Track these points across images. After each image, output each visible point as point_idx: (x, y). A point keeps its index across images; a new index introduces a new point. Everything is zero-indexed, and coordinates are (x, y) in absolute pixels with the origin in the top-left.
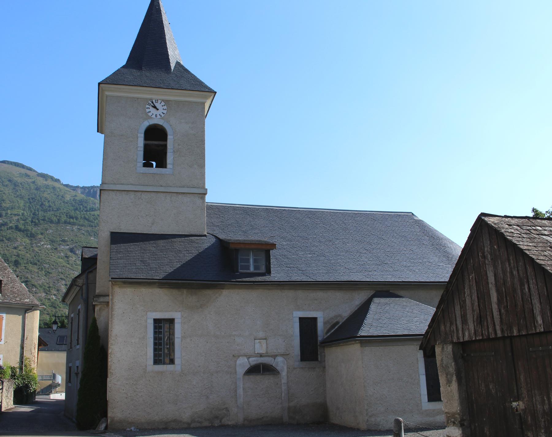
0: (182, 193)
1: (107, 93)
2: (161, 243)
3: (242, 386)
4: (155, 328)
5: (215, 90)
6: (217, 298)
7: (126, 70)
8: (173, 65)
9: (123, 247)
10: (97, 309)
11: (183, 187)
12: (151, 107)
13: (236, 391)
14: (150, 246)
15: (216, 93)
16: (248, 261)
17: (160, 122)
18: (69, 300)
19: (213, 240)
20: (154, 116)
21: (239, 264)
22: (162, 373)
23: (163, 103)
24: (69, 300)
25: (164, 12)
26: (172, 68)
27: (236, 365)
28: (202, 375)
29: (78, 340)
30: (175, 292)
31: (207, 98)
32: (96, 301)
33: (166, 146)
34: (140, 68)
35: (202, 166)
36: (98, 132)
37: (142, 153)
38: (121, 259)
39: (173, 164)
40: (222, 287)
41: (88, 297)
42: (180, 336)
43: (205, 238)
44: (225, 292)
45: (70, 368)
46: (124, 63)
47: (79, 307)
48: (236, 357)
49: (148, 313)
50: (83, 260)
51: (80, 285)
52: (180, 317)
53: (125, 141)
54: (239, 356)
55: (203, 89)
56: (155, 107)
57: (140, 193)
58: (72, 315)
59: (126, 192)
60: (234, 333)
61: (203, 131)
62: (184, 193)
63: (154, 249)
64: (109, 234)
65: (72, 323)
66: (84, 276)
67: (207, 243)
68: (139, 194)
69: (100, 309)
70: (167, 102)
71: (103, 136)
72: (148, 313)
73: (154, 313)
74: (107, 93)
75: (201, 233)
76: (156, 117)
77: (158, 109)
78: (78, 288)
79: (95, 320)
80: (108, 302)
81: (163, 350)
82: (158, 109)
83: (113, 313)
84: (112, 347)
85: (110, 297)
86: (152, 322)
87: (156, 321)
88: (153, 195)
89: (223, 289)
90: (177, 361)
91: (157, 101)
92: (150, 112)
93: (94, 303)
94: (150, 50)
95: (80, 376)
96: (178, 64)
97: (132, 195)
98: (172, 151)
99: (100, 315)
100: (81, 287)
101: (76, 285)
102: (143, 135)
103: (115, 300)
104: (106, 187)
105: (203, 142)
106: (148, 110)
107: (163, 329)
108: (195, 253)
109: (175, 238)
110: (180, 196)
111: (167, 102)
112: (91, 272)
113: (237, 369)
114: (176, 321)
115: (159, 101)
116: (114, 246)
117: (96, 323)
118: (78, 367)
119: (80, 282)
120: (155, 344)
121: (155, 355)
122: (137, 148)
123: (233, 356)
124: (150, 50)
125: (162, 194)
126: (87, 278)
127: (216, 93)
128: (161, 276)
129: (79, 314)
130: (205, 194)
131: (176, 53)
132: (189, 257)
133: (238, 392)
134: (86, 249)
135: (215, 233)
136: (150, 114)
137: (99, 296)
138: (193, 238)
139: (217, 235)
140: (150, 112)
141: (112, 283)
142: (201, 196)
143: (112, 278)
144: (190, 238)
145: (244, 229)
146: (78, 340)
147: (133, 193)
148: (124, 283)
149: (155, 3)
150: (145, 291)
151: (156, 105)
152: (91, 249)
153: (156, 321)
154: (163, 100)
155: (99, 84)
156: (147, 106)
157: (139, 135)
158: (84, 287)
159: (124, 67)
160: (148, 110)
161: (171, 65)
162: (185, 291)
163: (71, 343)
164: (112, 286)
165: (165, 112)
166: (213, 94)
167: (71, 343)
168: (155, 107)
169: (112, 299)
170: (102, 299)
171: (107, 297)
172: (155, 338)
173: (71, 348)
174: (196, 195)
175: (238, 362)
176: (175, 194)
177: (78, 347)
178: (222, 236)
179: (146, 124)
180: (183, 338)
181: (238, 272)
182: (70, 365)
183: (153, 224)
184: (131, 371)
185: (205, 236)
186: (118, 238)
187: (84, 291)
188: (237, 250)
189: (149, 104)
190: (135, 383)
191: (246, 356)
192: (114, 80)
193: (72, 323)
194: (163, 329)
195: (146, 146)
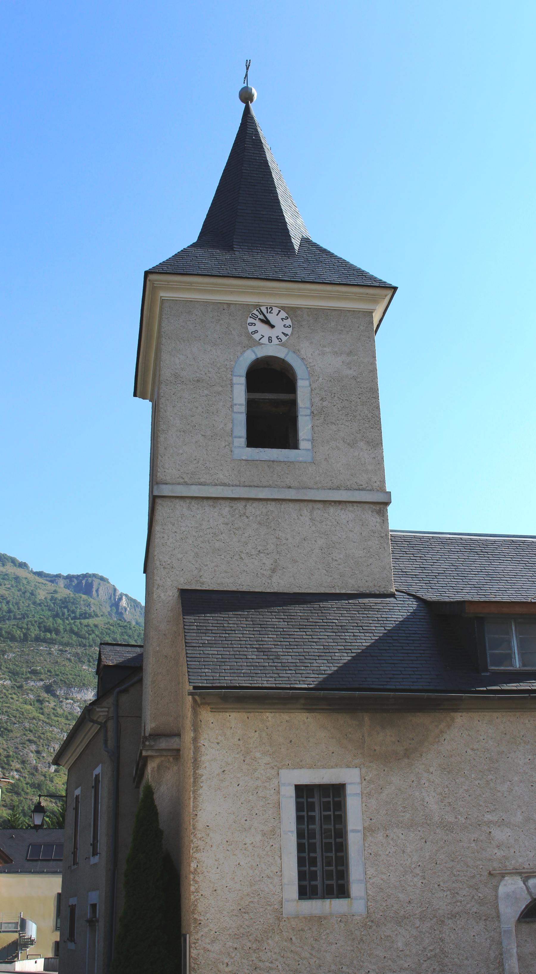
0: (335, 502)
1: (163, 294)
2: (297, 611)
3: (515, 950)
4: (299, 807)
5: (394, 284)
6: (442, 732)
7: (200, 252)
8: (296, 243)
9: (211, 619)
10: (151, 766)
11: (338, 488)
12: (257, 322)
13: (501, 964)
14: (273, 618)
15: (395, 289)
16: (509, 642)
17: (280, 353)
18: (71, 757)
19: (413, 605)
20: (265, 341)
21: (489, 652)
22: (319, 920)
23: (283, 314)
24: (71, 757)
25: (269, 147)
26: (296, 248)
27: (497, 897)
28: (418, 923)
29: (94, 845)
30: (343, 719)
31: (375, 300)
32: (151, 748)
33: (293, 403)
34: (229, 247)
35: (376, 443)
36: (135, 395)
37: (241, 419)
38: (210, 645)
39: (313, 441)
40: (454, 706)
41: (118, 747)
42: (360, 828)
43: (392, 599)
44: (461, 719)
45: (73, 909)
46: (195, 240)
47: (98, 770)
48: (496, 876)
49: (282, 772)
50: (103, 671)
51: (102, 720)
52: (358, 780)
53: (206, 392)
54: (503, 876)
55: (369, 283)
56: (266, 322)
57: (243, 503)
58: (78, 792)
59: (211, 502)
60: (488, 817)
61: (373, 371)
62: (340, 502)
63: (283, 624)
64: (176, 594)
65: (76, 809)
66: (110, 701)
67: (400, 610)
68: (240, 505)
69: (159, 767)
70: (291, 312)
71: (147, 405)
72: (282, 772)
73: (297, 772)
74: (163, 294)
75: (382, 590)
76: (271, 342)
77: (273, 327)
78: (96, 727)
79: (149, 792)
80: (178, 750)
81: (323, 865)
82: (273, 327)
83: (199, 772)
84: (197, 855)
85: (188, 735)
86: (292, 792)
87: (300, 790)
88: (271, 506)
89: (456, 710)
90: (356, 889)
91: (270, 309)
92: (256, 332)
93: (144, 753)
94: (246, 211)
95: (101, 926)
96: (306, 241)
97: (225, 508)
98: (308, 412)
99: (160, 778)
100: (103, 726)
101: (93, 721)
102: (243, 380)
103: (202, 741)
104: (166, 490)
105: (374, 392)
106: (251, 329)
107: (320, 812)
108: (380, 632)
109: (327, 600)
110: (332, 510)
111: (291, 312)
112: (125, 691)
113: (502, 907)
114: (349, 790)
115: (275, 310)
116: (190, 619)
117: (153, 801)
118: (94, 906)
119: (101, 713)
120: (300, 848)
121: (301, 876)
122: (232, 407)
123: (490, 874)
124: (246, 211)
125: (291, 505)
126: (117, 705)
127: (395, 289)
128: (312, 681)
129: (96, 788)
130: (387, 503)
131: (304, 218)
132: (365, 641)
133: (507, 967)
134: (108, 648)
135: (413, 590)
136: (257, 337)
137: (156, 736)
138: (366, 600)
139: (419, 594)
140: (256, 332)
141: (194, 700)
142: (377, 507)
143: (195, 688)
144: (361, 600)
145: (474, 582)
146: (94, 845)
147: (227, 503)
148: (225, 698)
149: (250, 131)
150: (271, 718)
151: (270, 317)
152: (118, 648)
153: (300, 790)
154: (283, 308)
155: (147, 273)
156: (250, 320)
157: (235, 380)
158: (111, 725)
159: (193, 245)
160: (251, 329)
161: (293, 241)
162: (367, 718)
163: (74, 853)
164: (194, 709)
165: (289, 331)
166: (390, 293)
167: (74, 853)
168: (266, 322)
169: (195, 740)
170: (163, 744)
171: (176, 739)
172: (300, 835)
173: (75, 863)
174: (367, 506)
175: (502, 890)
176: (320, 506)
177: (94, 860)
178: (430, 596)
179: (250, 356)
180: (368, 831)
181: (487, 670)
182: (73, 901)
183: (274, 571)
184: (246, 916)
185: (392, 595)
186: (196, 602)
187: (111, 734)
188: (481, 620)
189: (254, 317)
190: (254, 946)
191: (520, 874)
192: (176, 267)
193: (76, 809)
194: (320, 812)
195: (250, 403)
